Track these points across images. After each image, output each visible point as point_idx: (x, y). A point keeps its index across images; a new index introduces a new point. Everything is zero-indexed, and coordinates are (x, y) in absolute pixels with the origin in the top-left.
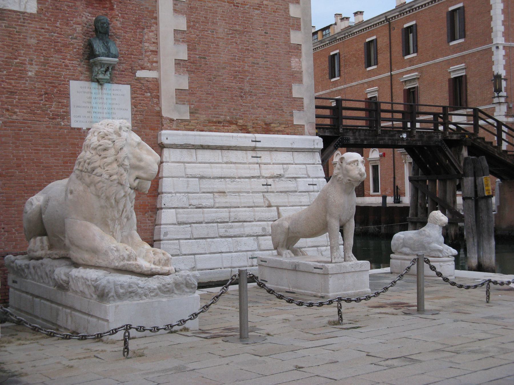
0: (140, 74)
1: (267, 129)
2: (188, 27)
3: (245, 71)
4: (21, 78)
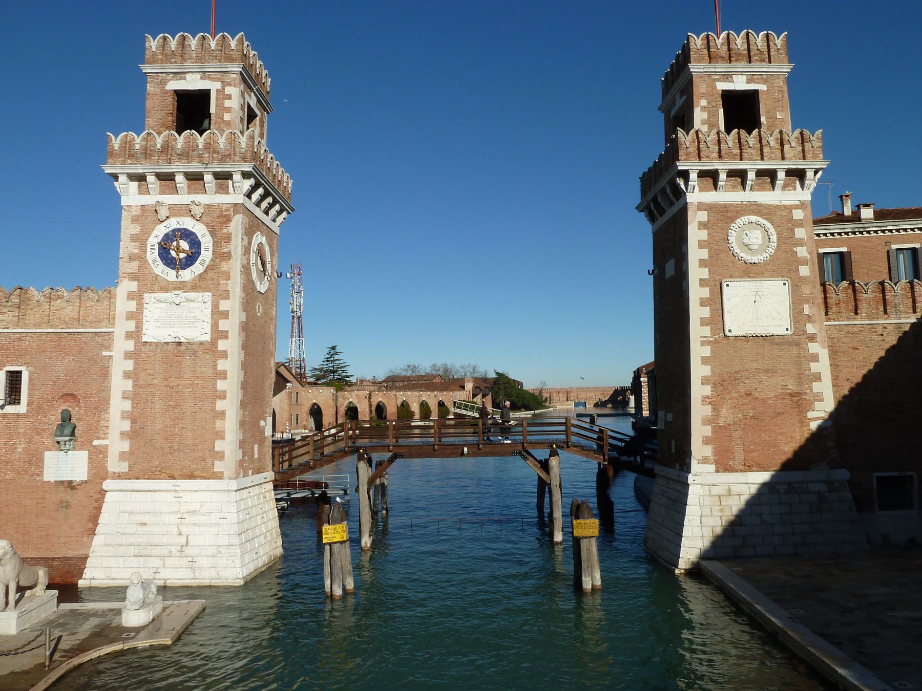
0: (95, 443)
1: (191, 477)
2: (133, 407)
3: (174, 435)
4: (13, 453)
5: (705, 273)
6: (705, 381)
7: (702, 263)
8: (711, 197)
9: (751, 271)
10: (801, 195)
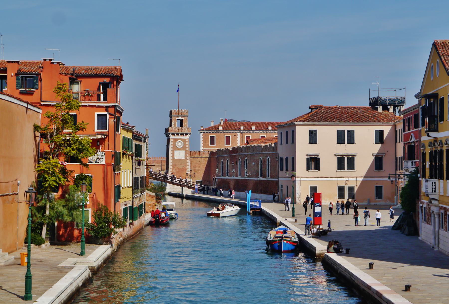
5: (172, 149)
6: (171, 166)
7: (172, 148)
8: (174, 137)
9: (179, 149)
10: (187, 137)
